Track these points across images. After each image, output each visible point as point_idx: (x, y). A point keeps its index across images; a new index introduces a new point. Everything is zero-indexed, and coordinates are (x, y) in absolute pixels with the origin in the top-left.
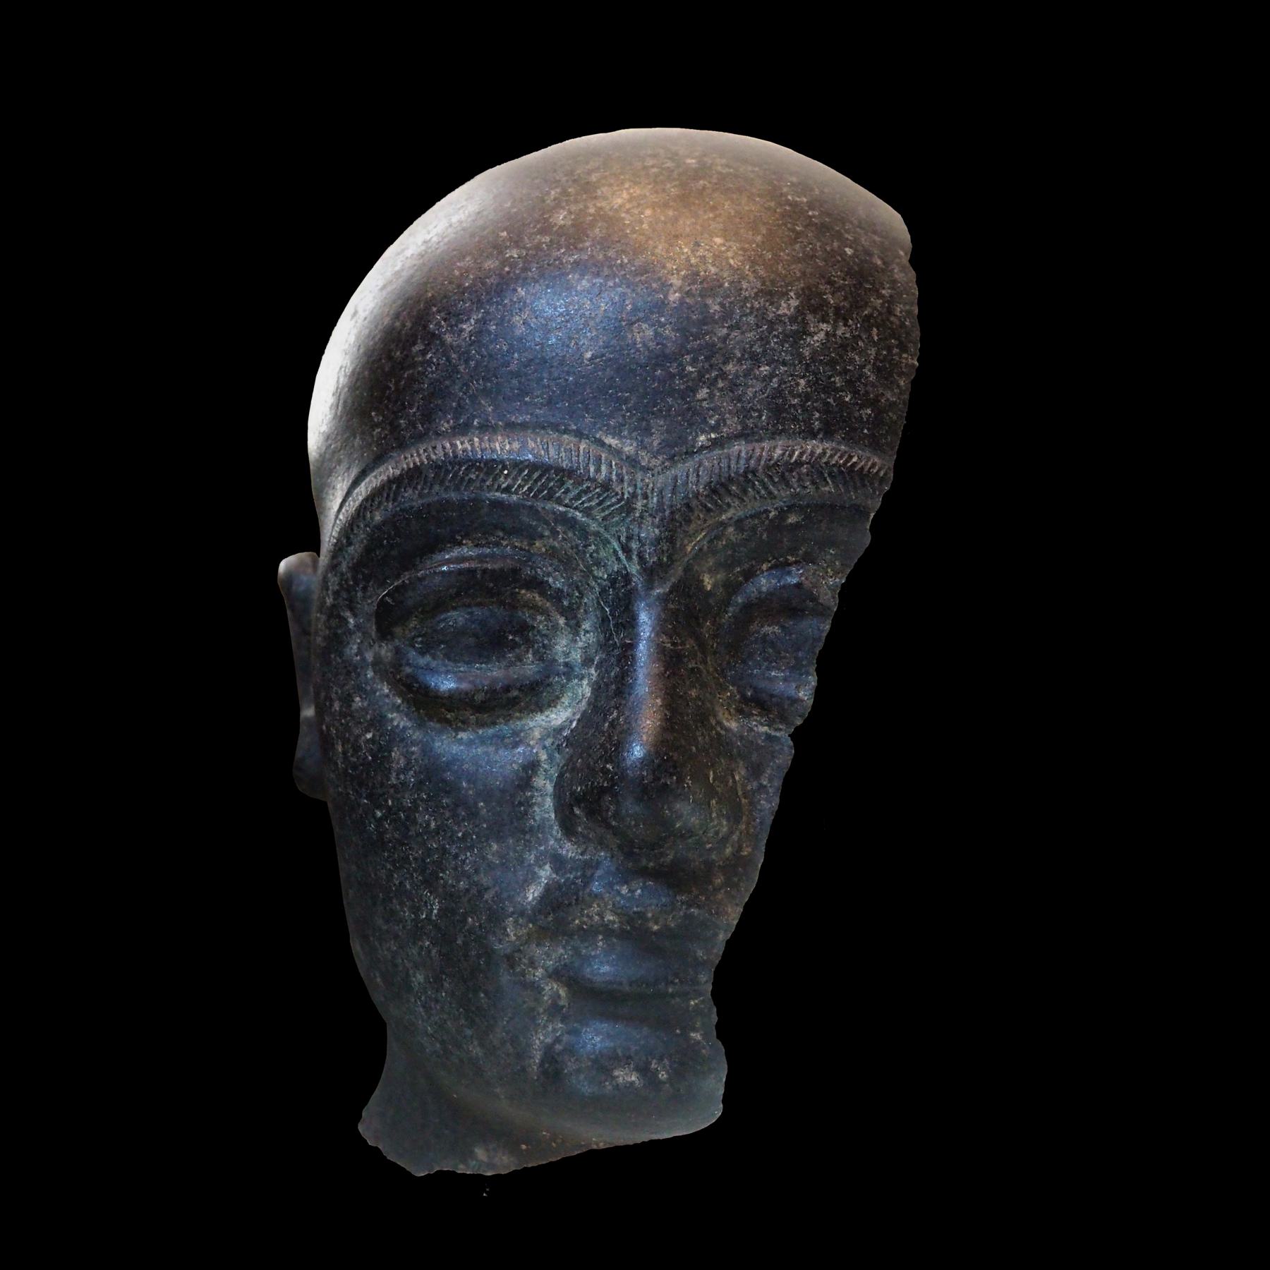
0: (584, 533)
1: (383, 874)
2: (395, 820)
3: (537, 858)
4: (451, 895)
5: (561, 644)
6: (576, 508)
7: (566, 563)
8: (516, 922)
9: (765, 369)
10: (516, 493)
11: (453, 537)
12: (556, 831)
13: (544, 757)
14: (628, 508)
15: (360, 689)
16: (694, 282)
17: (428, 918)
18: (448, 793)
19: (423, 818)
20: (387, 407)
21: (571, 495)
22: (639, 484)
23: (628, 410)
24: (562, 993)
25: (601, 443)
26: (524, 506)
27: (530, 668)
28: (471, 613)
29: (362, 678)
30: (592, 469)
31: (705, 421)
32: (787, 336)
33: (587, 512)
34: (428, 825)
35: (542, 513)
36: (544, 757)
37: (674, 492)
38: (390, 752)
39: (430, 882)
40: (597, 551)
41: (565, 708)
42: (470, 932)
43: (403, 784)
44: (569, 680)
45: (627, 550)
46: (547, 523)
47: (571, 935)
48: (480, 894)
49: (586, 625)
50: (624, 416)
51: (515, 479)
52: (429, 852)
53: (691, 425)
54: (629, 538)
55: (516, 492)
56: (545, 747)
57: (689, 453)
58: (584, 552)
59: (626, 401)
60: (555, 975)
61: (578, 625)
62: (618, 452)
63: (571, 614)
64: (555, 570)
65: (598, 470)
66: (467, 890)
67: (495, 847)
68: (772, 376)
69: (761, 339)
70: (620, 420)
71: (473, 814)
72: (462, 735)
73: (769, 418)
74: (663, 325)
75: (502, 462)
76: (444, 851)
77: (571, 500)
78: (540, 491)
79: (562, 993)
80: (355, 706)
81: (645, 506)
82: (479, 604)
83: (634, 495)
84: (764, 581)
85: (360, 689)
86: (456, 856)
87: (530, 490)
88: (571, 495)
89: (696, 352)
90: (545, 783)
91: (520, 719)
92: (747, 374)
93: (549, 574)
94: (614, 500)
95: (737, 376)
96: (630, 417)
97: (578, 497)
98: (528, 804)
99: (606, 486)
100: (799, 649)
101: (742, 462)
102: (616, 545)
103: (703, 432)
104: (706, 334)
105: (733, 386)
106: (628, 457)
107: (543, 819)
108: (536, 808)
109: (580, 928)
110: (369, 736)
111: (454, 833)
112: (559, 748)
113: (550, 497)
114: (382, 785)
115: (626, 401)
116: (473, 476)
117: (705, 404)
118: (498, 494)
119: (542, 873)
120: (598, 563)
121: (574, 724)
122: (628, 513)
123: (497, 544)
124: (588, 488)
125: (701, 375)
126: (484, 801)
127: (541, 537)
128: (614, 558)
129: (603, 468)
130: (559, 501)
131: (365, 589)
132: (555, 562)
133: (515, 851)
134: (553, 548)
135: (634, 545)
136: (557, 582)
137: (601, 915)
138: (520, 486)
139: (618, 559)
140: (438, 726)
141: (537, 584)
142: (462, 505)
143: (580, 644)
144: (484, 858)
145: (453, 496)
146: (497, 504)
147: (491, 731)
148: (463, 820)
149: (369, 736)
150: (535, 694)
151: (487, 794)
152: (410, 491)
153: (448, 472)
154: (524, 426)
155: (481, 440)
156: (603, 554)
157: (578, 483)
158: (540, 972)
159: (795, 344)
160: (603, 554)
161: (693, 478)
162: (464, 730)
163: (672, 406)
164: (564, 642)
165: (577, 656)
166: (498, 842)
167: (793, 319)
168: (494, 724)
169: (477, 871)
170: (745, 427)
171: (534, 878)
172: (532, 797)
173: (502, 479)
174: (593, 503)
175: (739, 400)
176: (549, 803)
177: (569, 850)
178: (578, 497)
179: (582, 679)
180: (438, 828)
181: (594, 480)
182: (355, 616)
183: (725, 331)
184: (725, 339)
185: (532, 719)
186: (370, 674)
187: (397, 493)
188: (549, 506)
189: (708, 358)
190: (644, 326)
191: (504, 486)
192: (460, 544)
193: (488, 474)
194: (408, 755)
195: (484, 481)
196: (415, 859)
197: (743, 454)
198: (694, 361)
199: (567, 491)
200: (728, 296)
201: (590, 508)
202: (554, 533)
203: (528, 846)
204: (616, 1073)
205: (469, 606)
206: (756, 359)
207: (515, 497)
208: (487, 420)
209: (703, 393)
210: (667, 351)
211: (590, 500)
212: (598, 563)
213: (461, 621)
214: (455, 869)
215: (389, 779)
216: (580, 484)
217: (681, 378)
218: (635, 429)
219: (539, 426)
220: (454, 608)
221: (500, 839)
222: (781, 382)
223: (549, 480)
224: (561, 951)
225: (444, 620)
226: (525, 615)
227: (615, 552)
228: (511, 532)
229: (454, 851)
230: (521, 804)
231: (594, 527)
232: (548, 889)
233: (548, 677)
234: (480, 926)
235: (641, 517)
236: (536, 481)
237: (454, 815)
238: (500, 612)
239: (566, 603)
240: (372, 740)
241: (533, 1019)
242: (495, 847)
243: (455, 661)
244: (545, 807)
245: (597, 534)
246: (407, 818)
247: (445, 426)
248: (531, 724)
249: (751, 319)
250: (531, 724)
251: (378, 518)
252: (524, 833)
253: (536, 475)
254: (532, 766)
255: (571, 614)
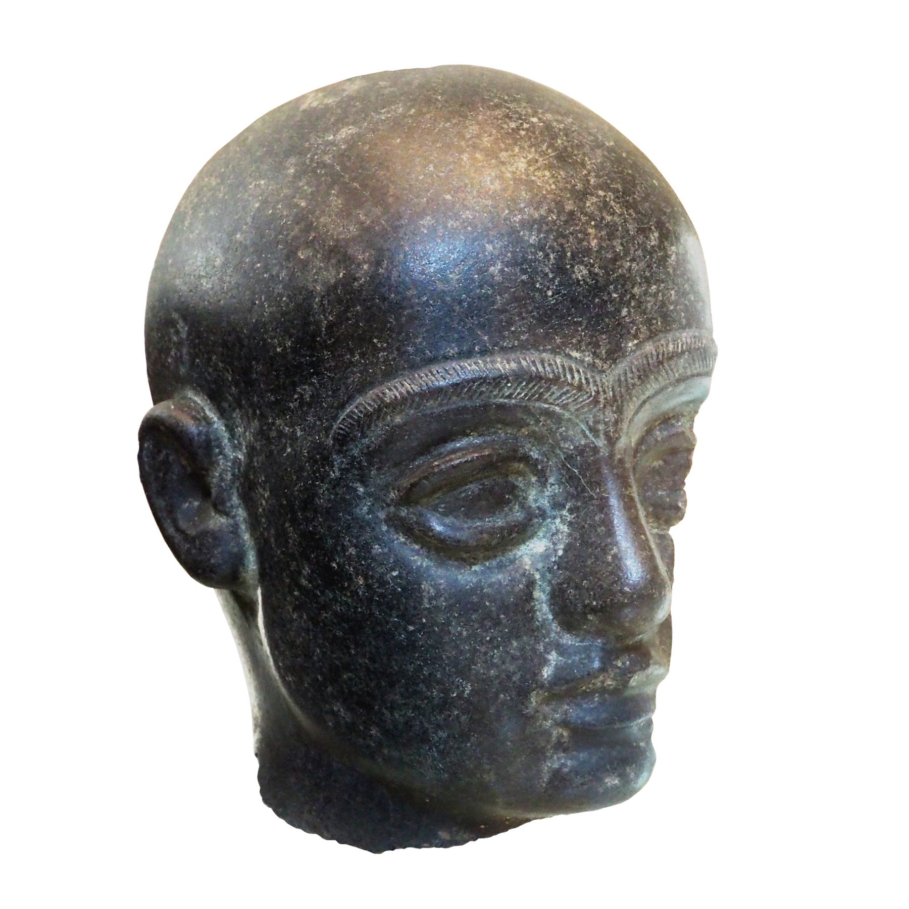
0: (558, 419)
1: (411, 668)
2: (428, 633)
3: (545, 649)
4: (483, 680)
5: (532, 494)
6: (558, 405)
7: (538, 439)
8: (538, 693)
9: (654, 287)
10: (515, 398)
11: (464, 431)
12: (555, 627)
13: (537, 576)
14: (596, 402)
15: (377, 540)
16: (601, 229)
17: (460, 696)
18: (476, 611)
19: (455, 629)
20: (391, 337)
21: (554, 397)
22: (599, 383)
23: (583, 331)
24: (565, 734)
25: (569, 357)
26: (520, 406)
27: (518, 515)
28: (483, 484)
29: (377, 530)
30: (569, 377)
31: (629, 333)
32: (660, 261)
33: (565, 407)
34: (460, 634)
35: (533, 410)
36: (537, 576)
37: (620, 386)
38: (420, 584)
39: (464, 672)
40: (566, 431)
41: (540, 539)
42: (503, 703)
43: (436, 607)
44: (544, 519)
45: (594, 431)
46: (533, 415)
47: (575, 697)
48: (509, 677)
49: (551, 480)
50: (581, 335)
51: (516, 389)
52: (461, 652)
53: (622, 336)
54: (597, 422)
55: (513, 395)
56: (537, 570)
57: (624, 356)
58: (556, 432)
59: (580, 324)
60: (557, 724)
61: (546, 480)
62: (582, 361)
63: (542, 477)
64: (533, 446)
65: (573, 378)
66: (497, 677)
67: (515, 644)
68: (658, 291)
69: (648, 266)
70: (579, 338)
71: (497, 623)
72: (474, 568)
73: (662, 323)
74: (592, 266)
75: (507, 377)
76: (476, 650)
77: (555, 400)
78: (533, 396)
79: (565, 734)
80: (374, 552)
81: (605, 399)
82: (486, 477)
83: (598, 392)
84: (658, 433)
85: (377, 540)
86: (486, 654)
87: (526, 395)
88: (554, 397)
89: (617, 280)
90: (541, 595)
91: (511, 550)
92: (646, 293)
93: (531, 450)
94: (585, 397)
95: (640, 296)
96: (585, 336)
97: (561, 396)
98: (532, 611)
99: (580, 388)
100: (675, 474)
101: (655, 358)
102: (584, 427)
103: (630, 340)
104: (619, 268)
105: (640, 303)
106: (589, 365)
107: (544, 620)
108: (538, 613)
109: (585, 691)
110: (395, 574)
111: (483, 638)
112: (550, 570)
113: (539, 399)
114: (415, 608)
115: (580, 324)
116: (484, 389)
117: (627, 320)
118: (501, 400)
119: (550, 657)
120: (565, 439)
121: (560, 553)
122: (595, 406)
123: (495, 433)
124: (568, 391)
125: (622, 296)
126: (504, 614)
127: (528, 425)
128: (581, 436)
129: (576, 375)
130: (546, 401)
131: (379, 469)
132: (532, 440)
133: (529, 645)
134: (534, 432)
135: (601, 427)
136: (535, 454)
137: (603, 682)
138: (519, 394)
139: (586, 436)
140: (456, 563)
141: (526, 459)
142: (475, 409)
143: (547, 493)
144: (508, 653)
145: (468, 403)
146: (501, 407)
147: (494, 563)
148: (490, 628)
149: (395, 574)
150: (521, 532)
151: (504, 608)
152: (431, 402)
153: (464, 387)
154: (513, 349)
155: (485, 362)
156: (571, 433)
157: (561, 388)
158: (549, 723)
159: (665, 267)
160: (571, 433)
161: (629, 375)
162: (475, 564)
163: (608, 325)
164: (534, 493)
165: (545, 503)
166: (516, 641)
167: (659, 247)
168: (495, 556)
169: (503, 663)
170: (651, 331)
171: (545, 662)
172: (535, 605)
173: (506, 389)
174: (570, 400)
175: (645, 313)
176: (545, 608)
177: (568, 640)
178: (561, 396)
179: (555, 518)
180: (469, 636)
181: (572, 385)
182: (366, 486)
183: (628, 264)
184: (630, 269)
185: (519, 550)
186: (385, 528)
187: (419, 405)
188: (537, 404)
189: (623, 286)
190: (581, 267)
191: (507, 394)
192: (468, 435)
193: (495, 387)
194: (436, 586)
195: (491, 392)
196: (448, 658)
197: (654, 352)
198: (616, 290)
199: (553, 393)
200: (623, 237)
201: (567, 404)
202: (538, 421)
203: (537, 640)
204: (606, 780)
205: (481, 479)
206: (648, 281)
207: (513, 401)
208: (485, 346)
209: (624, 312)
210: (599, 285)
211: (568, 399)
212: (565, 439)
213: (476, 491)
214: (486, 662)
215: (421, 604)
216: (562, 388)
217: (611, 303)
218: (590, 344)
219: (524, 347)
220: (471, 482)
221: (518, 637)
222: (663, 296)
223: (540, 387)
224: (566, 707)
225: (465, 491)
226: (511, 478)
227: (583, 431)
228: (505, 423)
229: (483, 649)
230: (529, 612)
231: (567, 415)
232: (557, 668)
233: (531, 520)
234: (512, 699)
235: (605, 407)
236: (531, 389)
237: (482, 626)
238: (500, 481)
239: (539, 467)
240: (400, 576)
241: (543, 753)
242: (515, 644)
243: (473, 519)
244: (543, 610)
245: (569, 420)
246: (442, 630)
247: (452, 351)
248: (519, 553)
249: (640, 253)
250: (519, 553)
251: (398, 420)
252: (533, 631)
253: (530, 386)
254: (531, 584)
255: (542, 477)
